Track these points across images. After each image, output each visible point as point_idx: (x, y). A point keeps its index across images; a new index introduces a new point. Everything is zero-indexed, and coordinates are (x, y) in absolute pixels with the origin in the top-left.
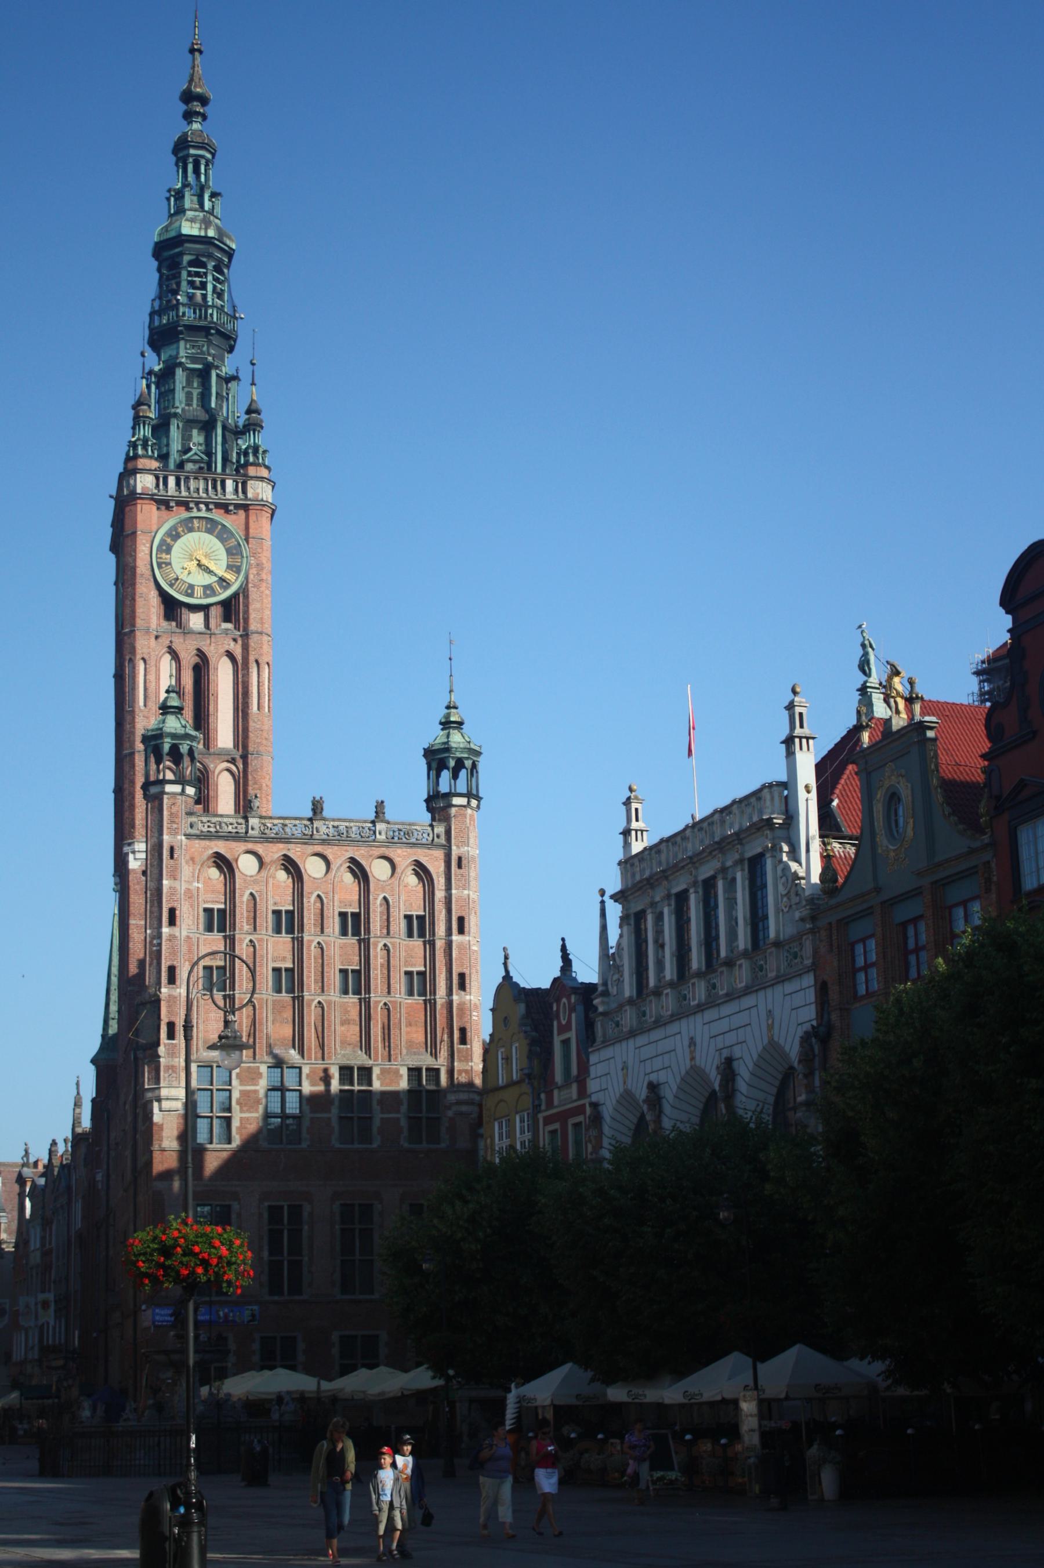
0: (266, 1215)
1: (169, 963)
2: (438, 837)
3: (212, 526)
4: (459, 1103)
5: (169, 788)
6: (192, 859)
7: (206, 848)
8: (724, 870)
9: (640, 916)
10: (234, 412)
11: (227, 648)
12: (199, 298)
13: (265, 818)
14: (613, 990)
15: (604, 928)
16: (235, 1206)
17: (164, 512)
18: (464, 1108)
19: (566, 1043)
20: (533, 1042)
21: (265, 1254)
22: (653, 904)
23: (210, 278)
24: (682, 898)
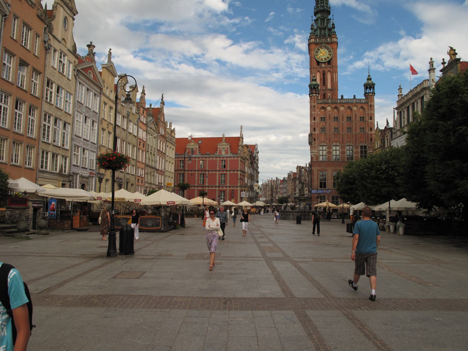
3: (325, 47)
5: (314, 95)
8: (416, 100)
9: (401, 112)
10: (330, 26)
14: (396, 128)
15: (394, 115)
19: (387, 139)
20: (382, 140)
22: (403, 110)
24: (408, 107)
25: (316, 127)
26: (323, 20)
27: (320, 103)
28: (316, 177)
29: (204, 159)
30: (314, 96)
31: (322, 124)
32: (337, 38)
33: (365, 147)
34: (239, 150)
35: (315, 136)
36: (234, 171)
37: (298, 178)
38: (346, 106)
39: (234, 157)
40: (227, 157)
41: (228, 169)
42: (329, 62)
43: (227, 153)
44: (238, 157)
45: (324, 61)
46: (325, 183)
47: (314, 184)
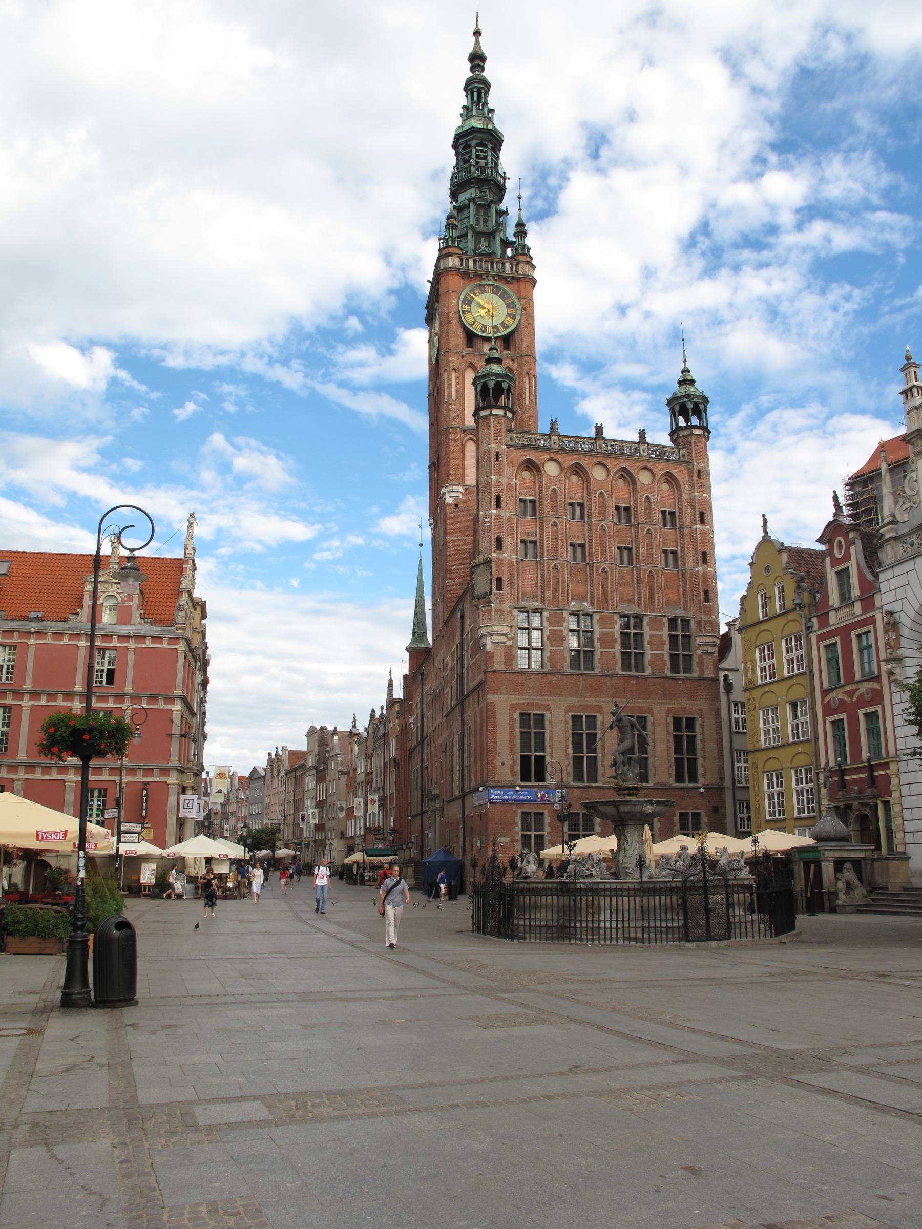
0: (570, 722)
1: (497, 535)
2: (683, 456)
3: (496, 290)
4: (705, 645)
5: (496, 412)
6: (512, 463)
7: (522, 455)
11: (508, 365)
12: (483, 165)
13: (563, 436)
16: (548, 715)
17: (466, 282)
18: (710, 649)
21: (571, 751)
23: (489, 153)
25: (504, 535)
26: (484, 208)
27: (519, 447)
28: (507, 737)
29: (15, 639)
30: (498, 416)
31: (527, 527)
32: (534, 267)
33: (686, 621)
34: (180, 609)
35: (499, 570)
36: (153, 699)
37: (316, 768)
38: (615, 465)
39: (157, 639)
40: (125, 637)
41: (128, 689)
42: (507, 341)
43: (124, 616)
44: (174, 639)
45: (489, 332)
46: (540, 761)
47: (498, 762)
